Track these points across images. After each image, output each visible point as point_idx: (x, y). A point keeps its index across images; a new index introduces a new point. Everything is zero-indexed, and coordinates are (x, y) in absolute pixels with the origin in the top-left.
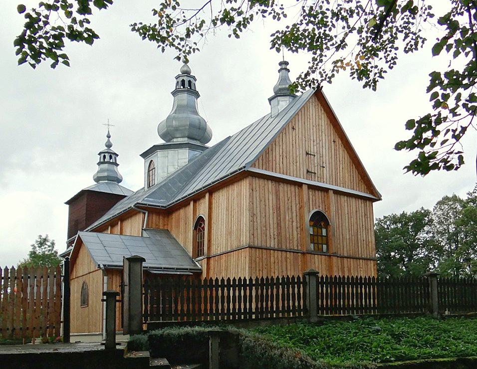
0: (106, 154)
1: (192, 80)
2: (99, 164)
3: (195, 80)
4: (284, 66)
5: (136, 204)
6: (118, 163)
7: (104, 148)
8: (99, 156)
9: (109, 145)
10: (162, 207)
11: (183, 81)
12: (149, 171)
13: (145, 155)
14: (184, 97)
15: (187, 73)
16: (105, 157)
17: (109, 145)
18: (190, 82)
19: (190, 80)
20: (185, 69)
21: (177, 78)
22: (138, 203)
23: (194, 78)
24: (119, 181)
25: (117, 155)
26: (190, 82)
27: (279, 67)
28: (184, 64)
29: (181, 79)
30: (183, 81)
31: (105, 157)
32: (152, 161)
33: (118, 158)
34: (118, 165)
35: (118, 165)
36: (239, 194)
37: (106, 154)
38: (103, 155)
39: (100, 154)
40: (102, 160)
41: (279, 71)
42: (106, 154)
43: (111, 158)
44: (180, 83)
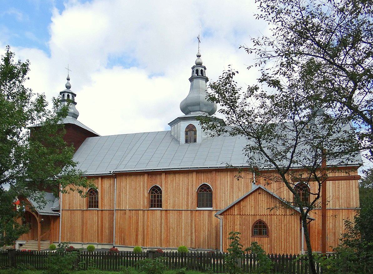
0: (70, 95)
6: (75, 101)
7: (64, 89)
9: (68, 87)
15: (199, 64)
16: (68, 96)
17: (68, 87)
18: (202, 71)
19: (202, 70)
20: (198, 61)
21: (193, 68)
25: (75, 95)
28: (197, 58)
29: (196, 68)
30: (197, 71)
31: (68, 96)
33: (75, 98)
37: (70, 94)
38: (62, 94)
44: (195, 72)
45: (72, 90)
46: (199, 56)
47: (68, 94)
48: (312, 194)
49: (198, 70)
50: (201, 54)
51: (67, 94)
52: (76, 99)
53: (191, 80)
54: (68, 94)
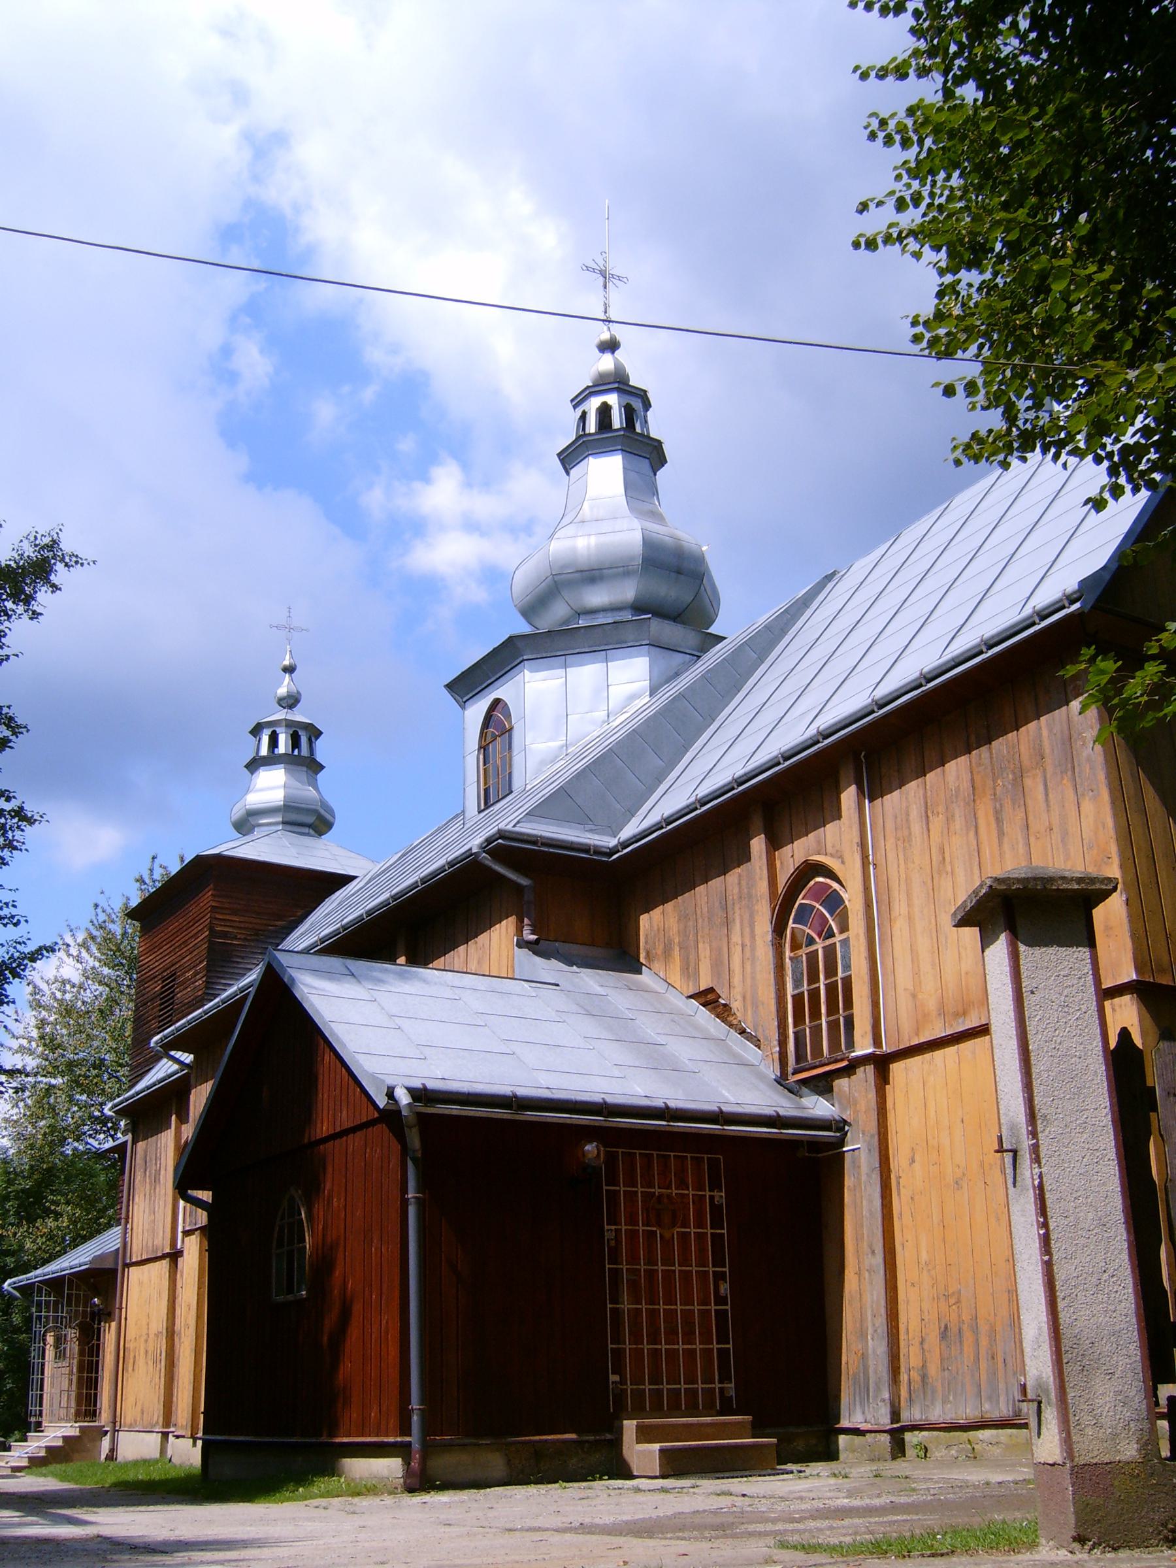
1: (637, 404)
3: (647, 405)
5: (489, 841)
6: (319, 758)
11: (605, 410)
15: (618, 381)
16: (274, 741)
22: (501, 834)
23: (642, 395)
25: (314, 733)
26: (630, 414)
29: (595, 403)
30: (605, 410)
31: (274, 741)
32: (497, 702)
33: (319, 744)
34: (322, 767)
35: (322, 767)
36: (1069, 741)
37: (278, 730)
40: (264, 751)
43: (295, 741)
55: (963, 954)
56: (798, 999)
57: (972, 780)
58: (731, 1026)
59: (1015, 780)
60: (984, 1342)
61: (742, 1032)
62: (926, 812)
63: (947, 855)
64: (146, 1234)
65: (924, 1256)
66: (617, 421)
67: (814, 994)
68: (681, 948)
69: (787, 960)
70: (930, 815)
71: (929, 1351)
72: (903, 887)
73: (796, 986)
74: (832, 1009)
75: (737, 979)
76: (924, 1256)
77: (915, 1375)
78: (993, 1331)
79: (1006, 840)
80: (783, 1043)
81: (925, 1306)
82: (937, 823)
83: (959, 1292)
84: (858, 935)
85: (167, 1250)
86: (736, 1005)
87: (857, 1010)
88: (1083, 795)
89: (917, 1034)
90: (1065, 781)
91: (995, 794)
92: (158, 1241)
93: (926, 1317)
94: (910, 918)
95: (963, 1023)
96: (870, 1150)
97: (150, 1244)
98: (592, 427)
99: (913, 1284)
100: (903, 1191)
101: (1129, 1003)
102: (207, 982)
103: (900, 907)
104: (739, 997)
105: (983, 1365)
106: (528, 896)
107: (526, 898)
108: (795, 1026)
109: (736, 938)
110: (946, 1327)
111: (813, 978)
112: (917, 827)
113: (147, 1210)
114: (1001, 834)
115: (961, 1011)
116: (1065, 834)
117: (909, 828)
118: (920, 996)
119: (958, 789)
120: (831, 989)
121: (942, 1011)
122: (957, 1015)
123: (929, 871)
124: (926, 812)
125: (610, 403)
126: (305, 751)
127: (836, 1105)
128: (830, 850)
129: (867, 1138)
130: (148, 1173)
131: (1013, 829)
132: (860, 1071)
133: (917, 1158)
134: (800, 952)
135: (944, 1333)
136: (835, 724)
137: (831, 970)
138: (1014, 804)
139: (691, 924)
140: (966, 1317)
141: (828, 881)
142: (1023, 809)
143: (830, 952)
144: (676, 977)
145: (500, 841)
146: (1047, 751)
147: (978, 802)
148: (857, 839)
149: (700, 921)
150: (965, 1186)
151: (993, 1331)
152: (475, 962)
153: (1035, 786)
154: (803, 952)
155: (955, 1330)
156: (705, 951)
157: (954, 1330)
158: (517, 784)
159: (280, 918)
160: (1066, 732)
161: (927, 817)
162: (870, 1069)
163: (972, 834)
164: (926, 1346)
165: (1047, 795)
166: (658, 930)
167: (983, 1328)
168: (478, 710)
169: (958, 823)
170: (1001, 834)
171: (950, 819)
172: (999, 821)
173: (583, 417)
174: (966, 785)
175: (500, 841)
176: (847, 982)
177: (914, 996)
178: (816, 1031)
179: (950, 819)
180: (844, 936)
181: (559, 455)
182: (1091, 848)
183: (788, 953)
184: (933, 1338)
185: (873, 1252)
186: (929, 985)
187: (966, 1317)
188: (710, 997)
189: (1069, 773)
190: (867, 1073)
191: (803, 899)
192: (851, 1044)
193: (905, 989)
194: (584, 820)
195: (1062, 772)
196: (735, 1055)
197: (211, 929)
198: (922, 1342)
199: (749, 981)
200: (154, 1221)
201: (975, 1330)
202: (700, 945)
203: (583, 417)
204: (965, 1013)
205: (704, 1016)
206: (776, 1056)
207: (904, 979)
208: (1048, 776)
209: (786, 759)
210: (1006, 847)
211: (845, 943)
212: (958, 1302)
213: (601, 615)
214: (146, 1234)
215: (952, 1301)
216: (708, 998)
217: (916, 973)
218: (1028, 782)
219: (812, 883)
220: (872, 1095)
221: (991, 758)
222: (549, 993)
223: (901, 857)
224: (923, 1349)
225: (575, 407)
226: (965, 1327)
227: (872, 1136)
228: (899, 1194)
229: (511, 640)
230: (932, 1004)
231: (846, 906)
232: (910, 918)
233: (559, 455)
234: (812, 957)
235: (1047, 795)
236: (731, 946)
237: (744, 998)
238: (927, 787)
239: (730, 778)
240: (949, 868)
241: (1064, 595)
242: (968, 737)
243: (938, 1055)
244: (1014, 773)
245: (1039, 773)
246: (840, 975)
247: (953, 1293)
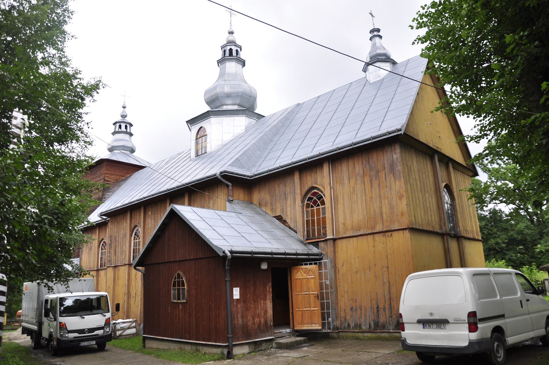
1: (239, 50)
2: (114, 133)
3: (241, 50)
4: (376, 33)
6: (132, 132)
7: (119, 119)
8: (114, 127)
9: (124, 116)
10: (248, 176)
11: (231, 50)
12: (197, 139)
13: (192, 122)
14: (231, 66)
16: (120, 127)
17: (124, 116)
18: (237, 51)
24: (132, 151)
25: (131, 125)
26: (237, 51)
27: (371, 35)
28: (229, 35)
29: (228, 48)
30: (231, 50)
31: (120, 127)
32: (201, 127)
34: (133, 135)
37: (122, 124)
38: (118, 125)
39: (114, 124)
41: (371, 39)
42: (122, 124)
43: (126, 127)
45: (128, 119)
46: (231, 33)
47: (120, 125)
48: (474, 240)
49: (232, 49)
50: (234, 29)
51: (125, 124)
52: (133, 130)
53: (220, 62)
54: (120, 125)
55: (359, 215)
56: (308, 221)
57: (363, 171)
58: (286, 226)
59: (376, 173)
60: (363, 312)
61: (290, 228)
62: (349, 177)
63: (355, 190)
64: (87, 263)
65: (346, 289)
66: (234, 53)
67: (313, 221)
68: (270, 204)
69: (305, 211)
70: (350, 178)
71: (347, 313)
72: (342, 196)
73: (307, 218)
74: (319, 225)
75: (289, 214)
76: (346, 289)
77: (343, 319)
78: (366, 309)
79: (373, 188)
80: (304, 232)
81: (346, 302)
82: (353, 181)
83: (356, 299)
84: (328, 207)
85: (96, 269)
86: (288, 221)
87: (328, 226)
88: (396, 179)
89: (345, 234)
90: (391, 175)
91: (370, 176)
92: (92, 266)
93: (346, 304)
94: (343, 204)
95: (359, 232)
96: (331, 262)
97: (89, 266)
98: (227, 54)
99: (342, 296)
100: (340, 273)
101: (408, 232)
102: (103, 194)
103: (341, 201)
104: (290, 219)
105: (363, 317)
106: (230, 188)
107: (230, 189)
108: (307, 228)
109: (289, 202)
110: (352, 307)
111: (313, 216)
112: (346, 181)
113: (88, 257)
114: (372, 186)
115: (358, 229)
116: (391, 188)
117: (344, 181)
118: (346, 224)
119: (359, 173)
120: (318, 220)
121: (352, 228)
122: (357, 230)
123: (349, 193)
124: (349, 177)
125: (232, 48)
126: (128, 131)
127: (320, 249)
128: (319, 184)
129: (331, 259)
130: (88, 247)
131: (375, 185)
132: (328, 242)
133: (344, 265)
134: (309, 209)
135: (352, 309)
136: (325, 152)
137: (318, 215)
138: (376, 178)
139: (274, 198)
140: (358, 305)
141: (318, 192)
142: (378, 180)
143: (318, 210)
144: (269, 211)
145: (225, 173)
146: (386, 166)
147: (365, 177)
148: (329, 182)
149: (277, 197)
150: (358, 273)
151: (366, 309)
152: (212, 204)
153: (382, 175)
154: (310, 209)
155: (355, 308)
156: (278, 205)
157: (354, 308)
158: (208, 150)
159: (123, 176)
160: (392, 162)
161: (349, 179)
162: (332, 241)
163: (363, 185)
164: (346, 312)
165: (386, 178)
166: (263, 198)
167: (363, 308)
168: (195, 128)
169: (359, 181)
170: (372, 186)
171: (356, 180)
172: (371, 183)
173: (225, 51)
174: (361, 172)
175: (225, 173)
176: (324, 219)
177: (344, 224)
178: (314, 230)
179: (356, 180)
180: (323, 206)
181: (217, 61)
182: (398, 193)
183: (305, 209)
184: (348, 310)
185: (332, 288)
186: (348, 222)
187: (358, 305)
188: (280, 218)
189: (392, 173)
190: (330, 243)
191: (310, 195)
192: (325, 234)
193: (342, 222)
194: (243, 167)
195: (390, 173)
196: (289, 234)
197: (104, 179)
198: (345, 311)
199: (292, 215)
200: (90, 260)
201: (361, 309)
202: (277, 204)
203: (225, 51)
204: (359, 230)
205: (277, 222)
206: (302, 236)
207: (341, 220)
208: (386, 173)
209: (309, 159)
210: (373, 189)
211: (324, 209)
212: (356, 301)
213: (229, 106)
214: (87, 263)
215: (354, 301)
216: (279, 218)
217: (345, 218)
218: (380, 174)
219: (313, 191)
220: (332, 249)
221: (369, 166)
222: (240, 216)
223: (341, 189)
224: (345, 313)
225: (222, 48)
226: (358, 308)
227: (332, 259)
228: (339, 274)
229: (208, 111)
230: (349, 227)
231: (323, 200)
232: (343, 204)
233: (217, 61)
234: (313, 211)
235: (386, 178)
236: (287, 205)
237: (291, 220)
238: (350, 171)
239: (291, 162)
240: (356, 193)
241: (397, 129)
242: (362, 160)
243: (351, 239)
244: (376, 171)
245: (384, 172)
246: (321, 216)
247: (354, 300)
